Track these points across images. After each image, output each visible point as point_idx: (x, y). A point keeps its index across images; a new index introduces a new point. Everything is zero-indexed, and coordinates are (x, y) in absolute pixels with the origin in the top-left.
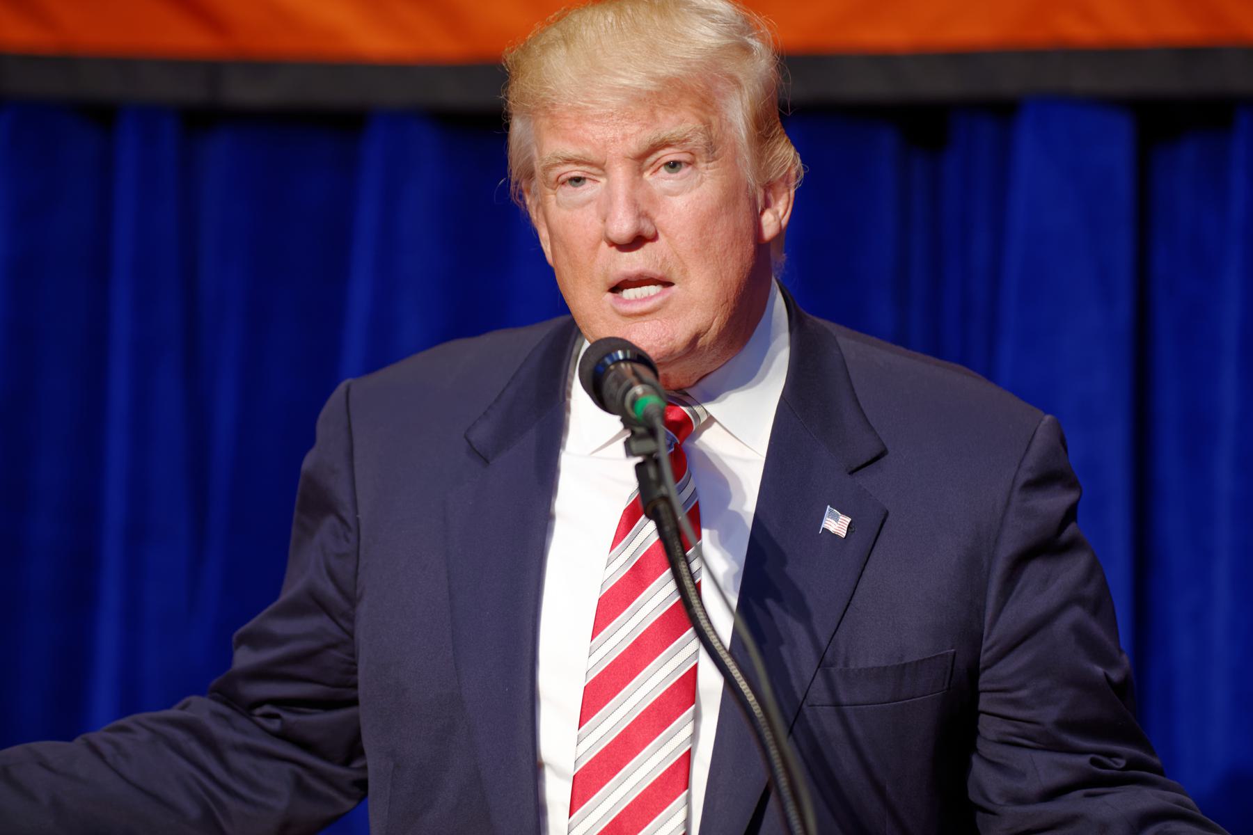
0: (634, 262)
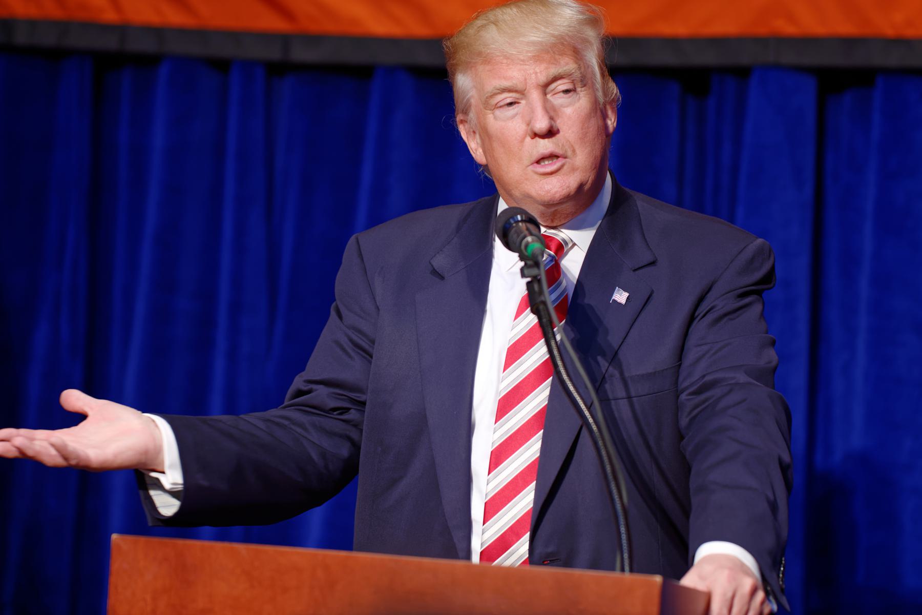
0: (545, 146)
